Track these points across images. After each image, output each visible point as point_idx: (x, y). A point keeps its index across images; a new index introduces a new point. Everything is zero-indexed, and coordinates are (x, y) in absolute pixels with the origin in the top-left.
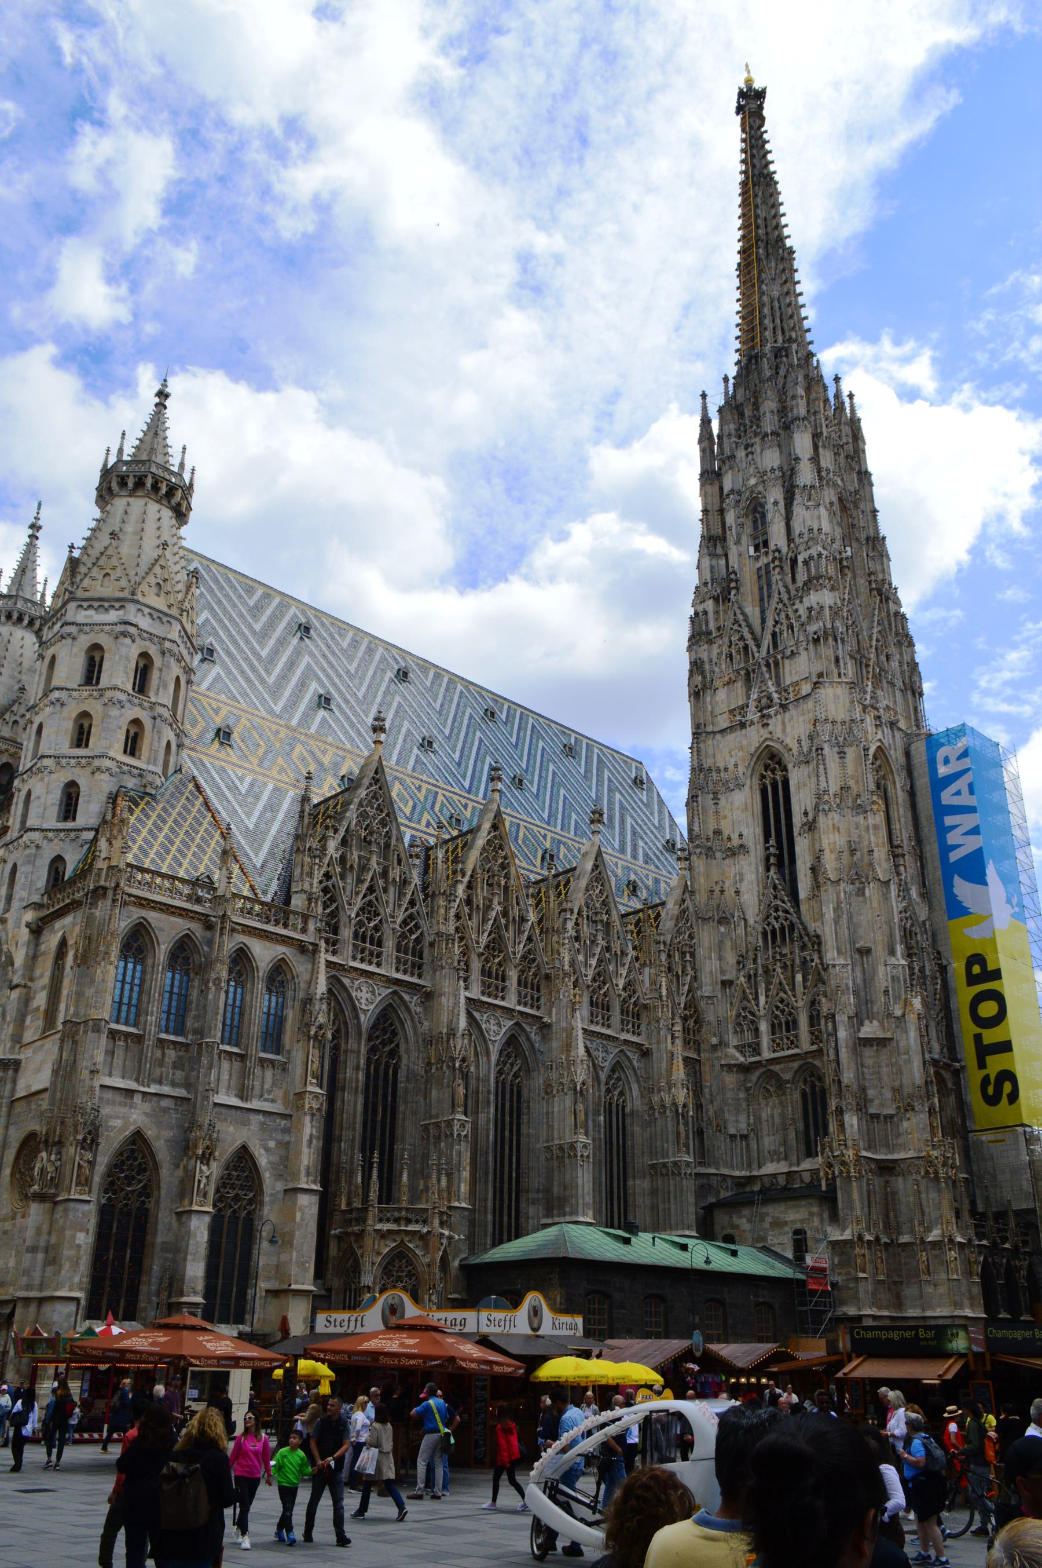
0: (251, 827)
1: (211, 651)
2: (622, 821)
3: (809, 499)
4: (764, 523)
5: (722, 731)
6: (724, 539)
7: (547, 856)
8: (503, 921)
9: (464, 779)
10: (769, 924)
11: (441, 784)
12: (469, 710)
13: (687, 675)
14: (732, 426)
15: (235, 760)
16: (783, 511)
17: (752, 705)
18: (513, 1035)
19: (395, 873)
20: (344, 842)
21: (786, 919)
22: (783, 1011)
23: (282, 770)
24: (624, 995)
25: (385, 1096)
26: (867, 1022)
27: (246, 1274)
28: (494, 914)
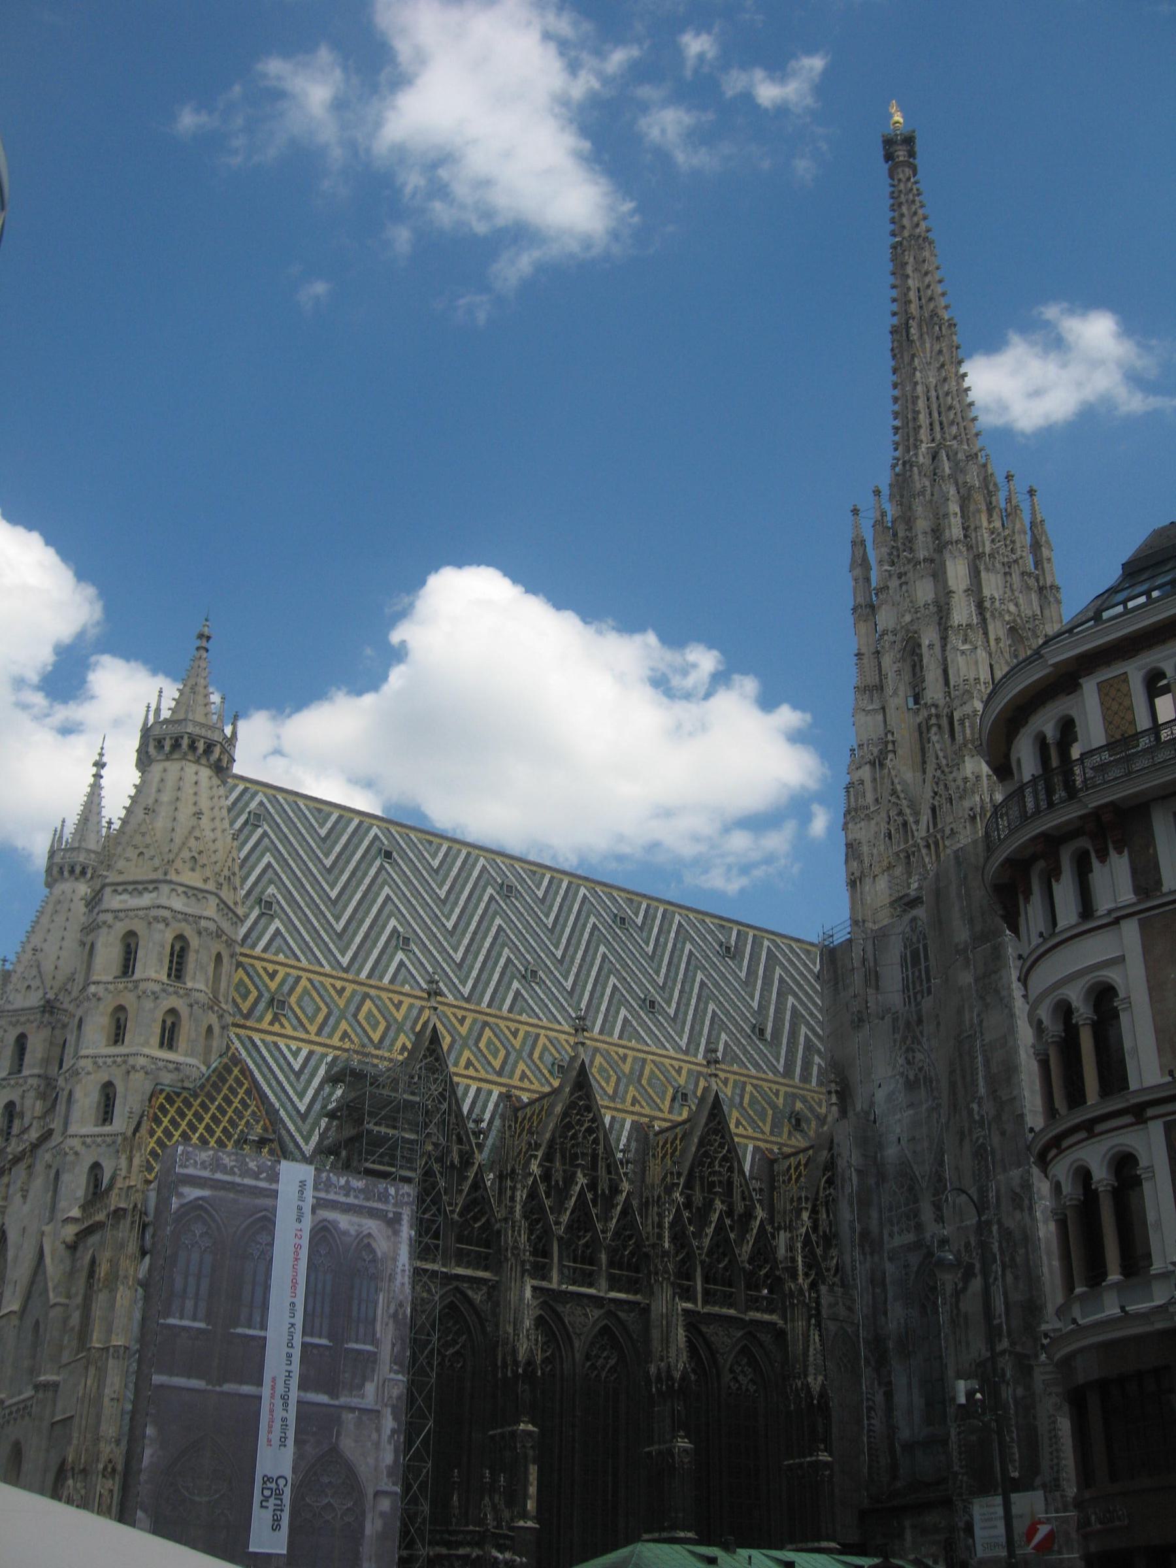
0: (303, 1109)
1: (269, 905)
2: (793, 1034)
3: (965, 641)
4: (922, 667)
6: (882, 688)
11: (545, 1022)
12: (592, 919)
13: (844, 858)
14: (885, 550)
15: (289, 1031)
16: (940, 657)
18: (606, 1327)
23: (345, 1035)
28: (578, 1188)
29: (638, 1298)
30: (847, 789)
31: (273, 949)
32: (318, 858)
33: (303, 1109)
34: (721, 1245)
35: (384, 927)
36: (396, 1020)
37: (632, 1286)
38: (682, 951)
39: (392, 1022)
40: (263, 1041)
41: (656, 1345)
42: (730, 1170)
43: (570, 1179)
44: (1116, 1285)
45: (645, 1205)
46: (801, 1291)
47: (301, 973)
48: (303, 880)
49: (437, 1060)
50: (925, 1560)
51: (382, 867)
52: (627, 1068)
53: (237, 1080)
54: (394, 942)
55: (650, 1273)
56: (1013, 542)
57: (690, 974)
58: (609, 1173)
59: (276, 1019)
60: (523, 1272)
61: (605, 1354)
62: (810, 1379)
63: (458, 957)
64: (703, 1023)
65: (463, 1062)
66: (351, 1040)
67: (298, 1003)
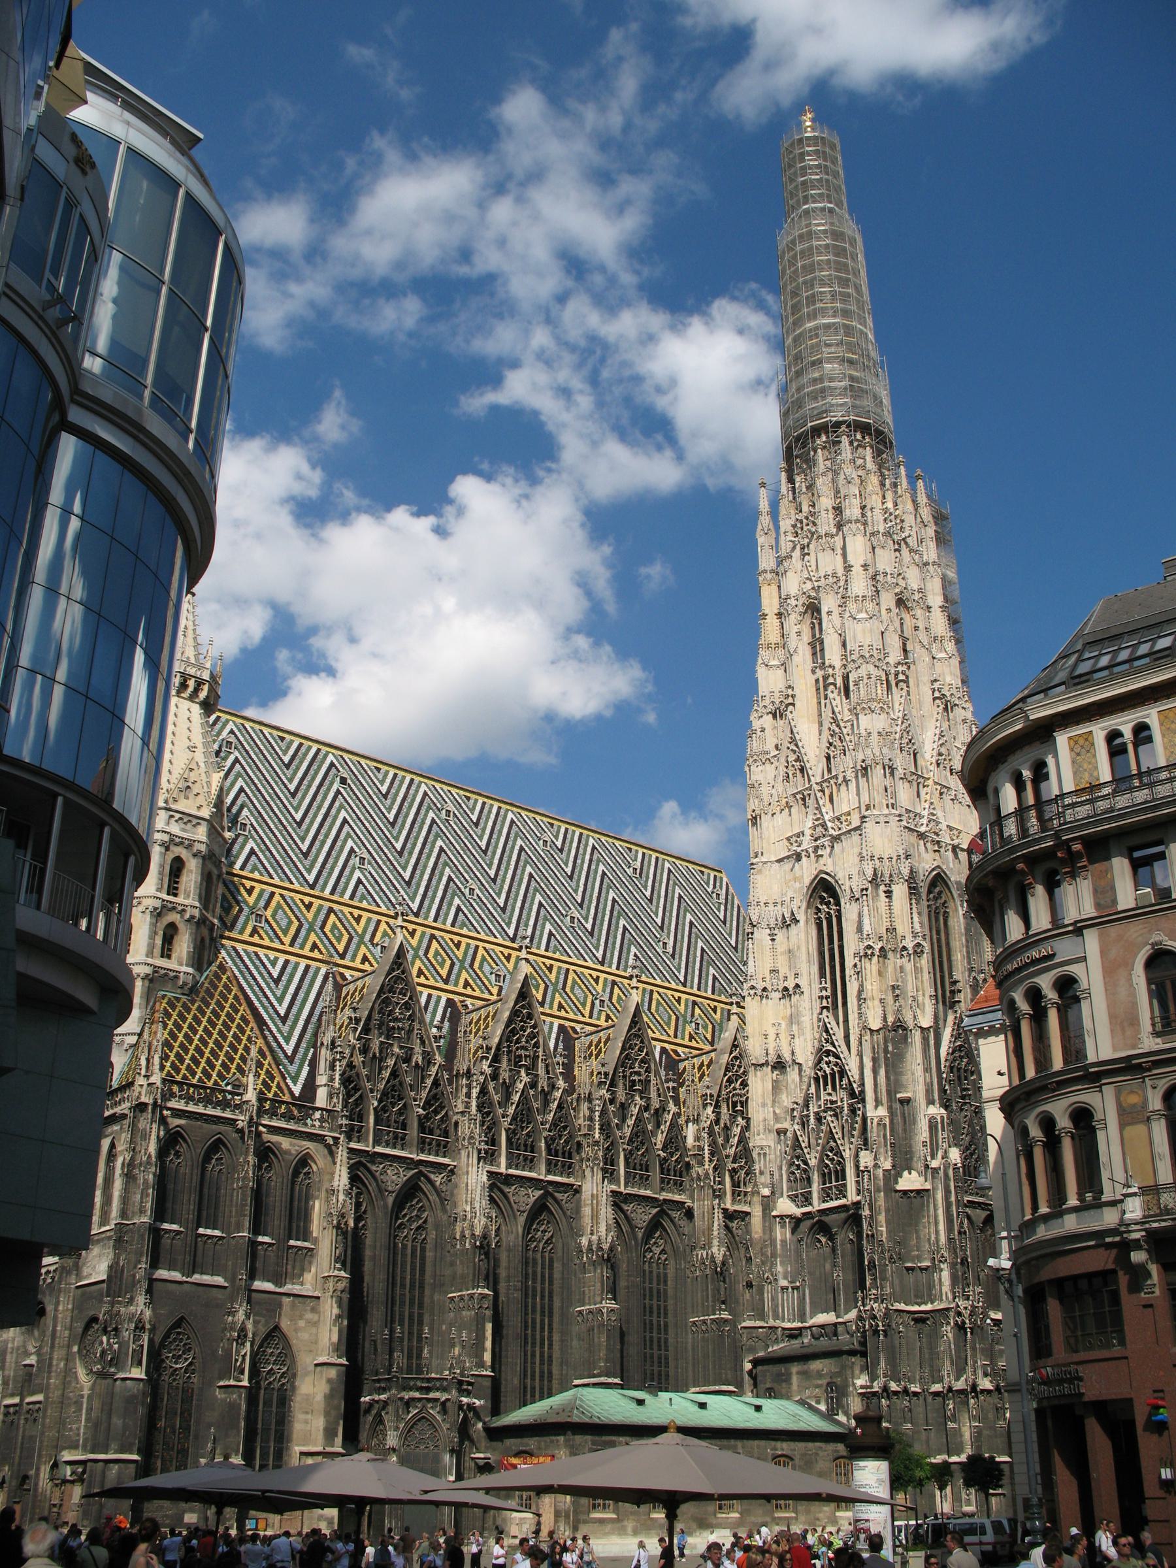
0: (282, 1013)
5: (779, 861)
7: (597, 1002)
8: (532, 1092)
9: (509, 927)
11: (482, 936)
12: (519, 842)
15: (267, 942)
17: (808, 832)
19: (418, 1058)
20: (366, 1030)
21: (836, 1064)
22: (832, 1160)
23: (314, 947)
24: (662, 1154)
25: (413, 1269)
26: (906, 1173)
27: (282, 1437)
28: (520, 1086)
29: (571, 1180)
31: (249, 867)
32: (283, 783)
33: (282, 1013)
34: (640, 1136)
35: (343, 847)
36: (355, 930)
37: (568, 1169)
38: (596, 871)
39: (353, 934)
40: (245, 951)
41: (587, 1221)
42: (648, 1070)
44: (1075, 1210)
46: (707, 1174)
47: (274, 889)
48: (272, 803)
49: (403, 972)
51: (338, 792)
52: (553, 977)
53: (226, 986)
54: (351, 863)
55: (582, 1160)
56: (902, 521)
57: (604, 891)
58: (548, 1072)
59: (255, 931)
60: (479, 1159)
62: (715, 1250)
63: (407, 876)
64: (615, 937)
65: (414, 972)
67: (273, 916)
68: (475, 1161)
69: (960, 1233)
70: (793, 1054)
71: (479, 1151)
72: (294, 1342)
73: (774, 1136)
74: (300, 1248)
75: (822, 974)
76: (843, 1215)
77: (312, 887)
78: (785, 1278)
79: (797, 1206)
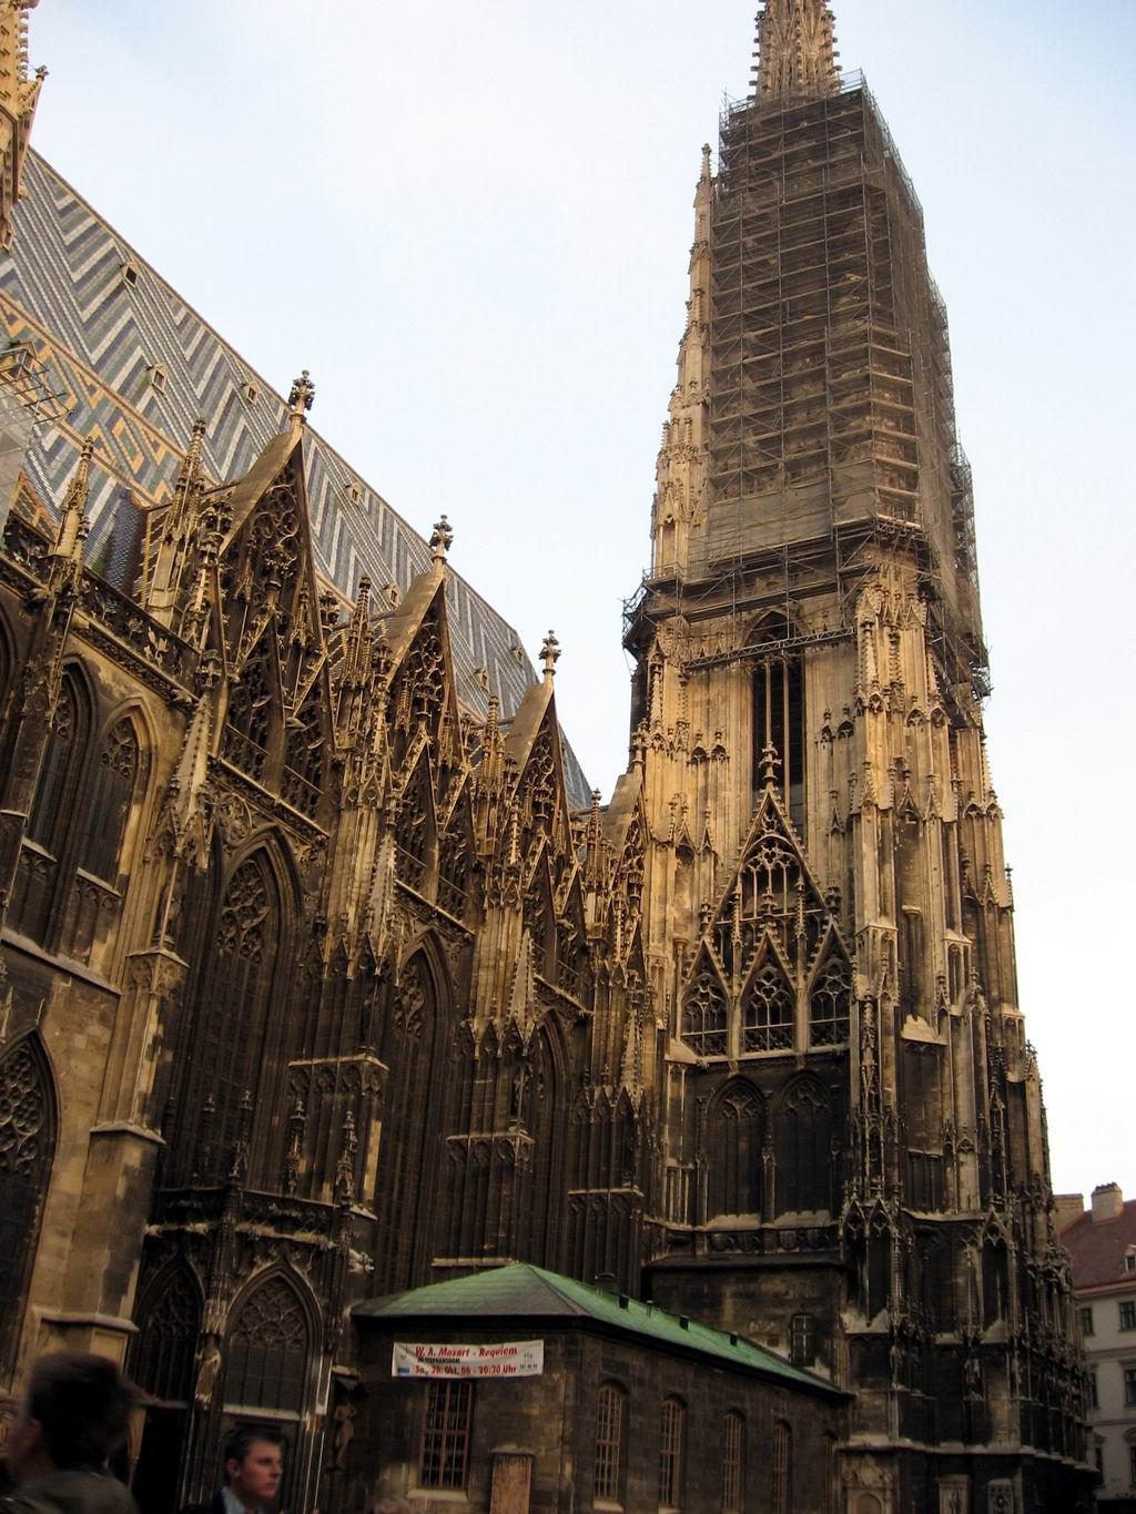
10: (756, 863)
12: (326, 478)
13: (651, 502)
19: (299, 634)
21: (785, 859)
22: (768, 992)
26: (910, 1018)
28: (421, 747)
29: (460, 922)
30: (667, 426)
34: (542, 888)
35: (131, 350)
42: (553, 797)
43: (414, 729)
45: (481, 801)
47: (46, 341)
49: (294, 490)
50: (754, 1340)
54: (142, 372)
60: (382, 829)
61: (411, 991)
62: (629, 1086)
66: (106, 452)
68: (372, 832)
69: (992, 1113)
70: (707, 838)
71: (382, 813)
72: (61, 1076)
73: (670, 947)
74: (96, 889)
75: (758, 741)
76: (783, 1072)
77: (96, 368)
78: (673, 1155)
79: (699, 1054)
